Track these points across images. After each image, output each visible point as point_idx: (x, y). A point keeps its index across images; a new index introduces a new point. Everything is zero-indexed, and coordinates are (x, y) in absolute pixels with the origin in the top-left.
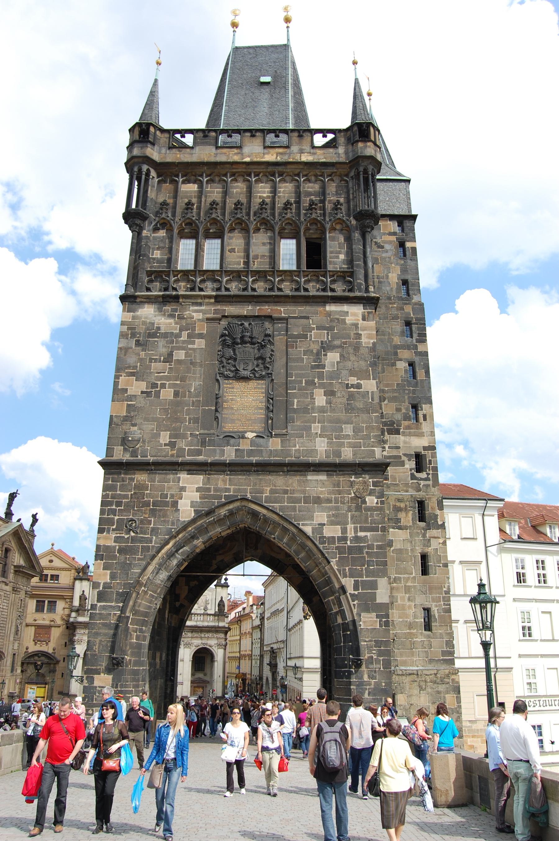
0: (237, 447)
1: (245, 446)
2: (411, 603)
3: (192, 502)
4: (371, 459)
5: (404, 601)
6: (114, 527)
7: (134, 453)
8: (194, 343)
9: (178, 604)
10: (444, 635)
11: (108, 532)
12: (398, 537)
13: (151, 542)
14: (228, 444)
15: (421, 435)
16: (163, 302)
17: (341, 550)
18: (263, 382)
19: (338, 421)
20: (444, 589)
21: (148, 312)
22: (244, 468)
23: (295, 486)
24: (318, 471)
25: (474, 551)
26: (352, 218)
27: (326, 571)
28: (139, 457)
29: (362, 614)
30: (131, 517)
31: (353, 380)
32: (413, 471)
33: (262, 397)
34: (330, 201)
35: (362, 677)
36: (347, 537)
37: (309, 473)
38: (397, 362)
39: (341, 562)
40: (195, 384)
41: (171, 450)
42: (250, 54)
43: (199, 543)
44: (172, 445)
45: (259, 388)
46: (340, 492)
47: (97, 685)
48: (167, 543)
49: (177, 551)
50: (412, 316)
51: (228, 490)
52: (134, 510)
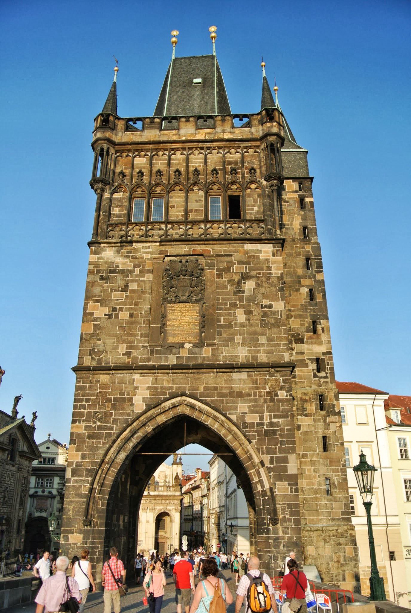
1: (184, 353)
2: (316, 474)
3: (144, 398)
5: (311, 472)
6: (84, 418)
8: (144, 276)
9: (137, 478)
10: (342, 498)
12: (304, 422)
13: (112, 430)
14: (171, 353)
15: (320, 343)
16: (121, 246)
17: (259, 433)
19: (255, 333)
20: (342, 463)
21: (109, 254)
22: (184, 371)
23: (224, 384)
24: (241, 372)
25: (367, 433)
26: (263, 179)
27: (248, 450)
28: (103, 364)
29: (277, 483)
30: (97, 410)
32: (315, 371)
33: (196, 316)
34: (246, 168)
35: (277, 533)
38: (301, 288)
39: (261, 442)
40: (145, 307)
42: (186, 63)
43: (149, 429)
44: (128, 354)
45: (194, 310)
46: (257, 388)
47: (71, 542)
48: (125, 430)
49: (132, 436)
51: (171, 388)
52: (99, 405)
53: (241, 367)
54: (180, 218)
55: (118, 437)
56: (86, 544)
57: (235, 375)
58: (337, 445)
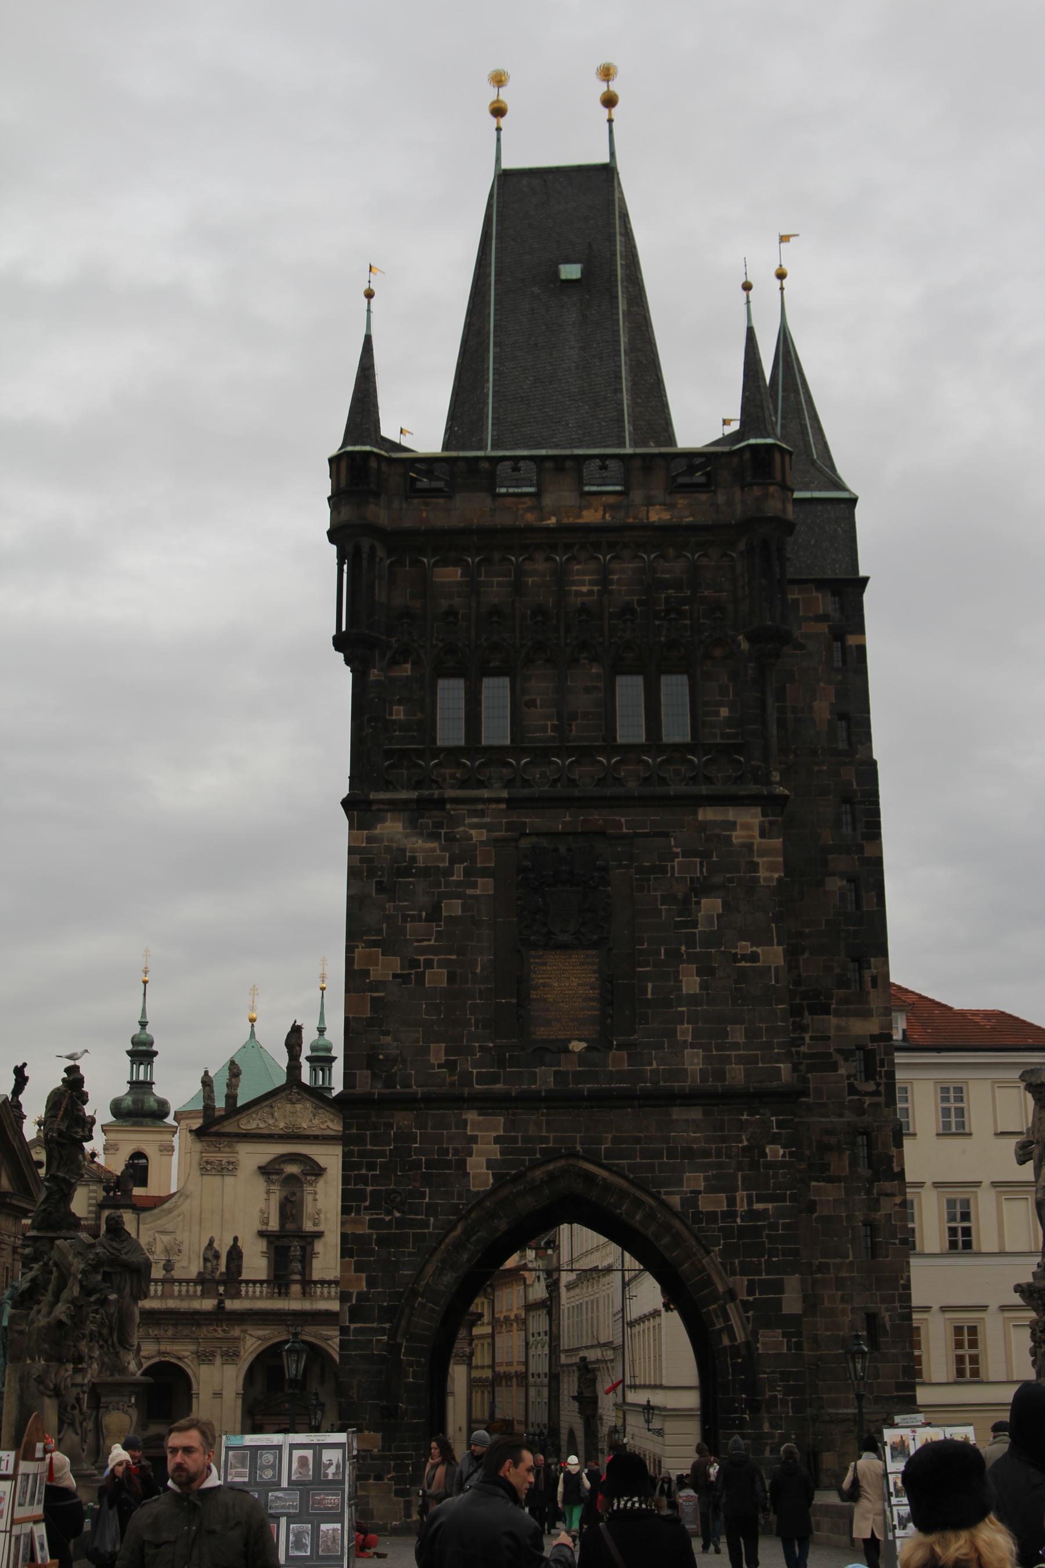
0: (556, 1068)
3: (488, 1161)
4: (775, 1084)
6: (367, 1204)
7: (390, 1082)
8: (474, 885)
11: (358, 1212)
12: (826, 1195)
15: (866, 1014)
18: (594, 952)
20: (902, 1282)
26: (741, 637)
29: (761, 1331)
31: (745, 947)
36: (736, 1212)
37: (676, 1108)
40: (481, 961)
41: (450, 1075)
44: (450, 1065)
48: (453, 1228)
50: (855, 787)
51: (545, 1140)
52: (396, 1175)
53: (688, 1098)
54: (550, 733)
55: (440, 1244)
56: (389, 1450)
57: (677, 1113)
58: (894, 1244)
